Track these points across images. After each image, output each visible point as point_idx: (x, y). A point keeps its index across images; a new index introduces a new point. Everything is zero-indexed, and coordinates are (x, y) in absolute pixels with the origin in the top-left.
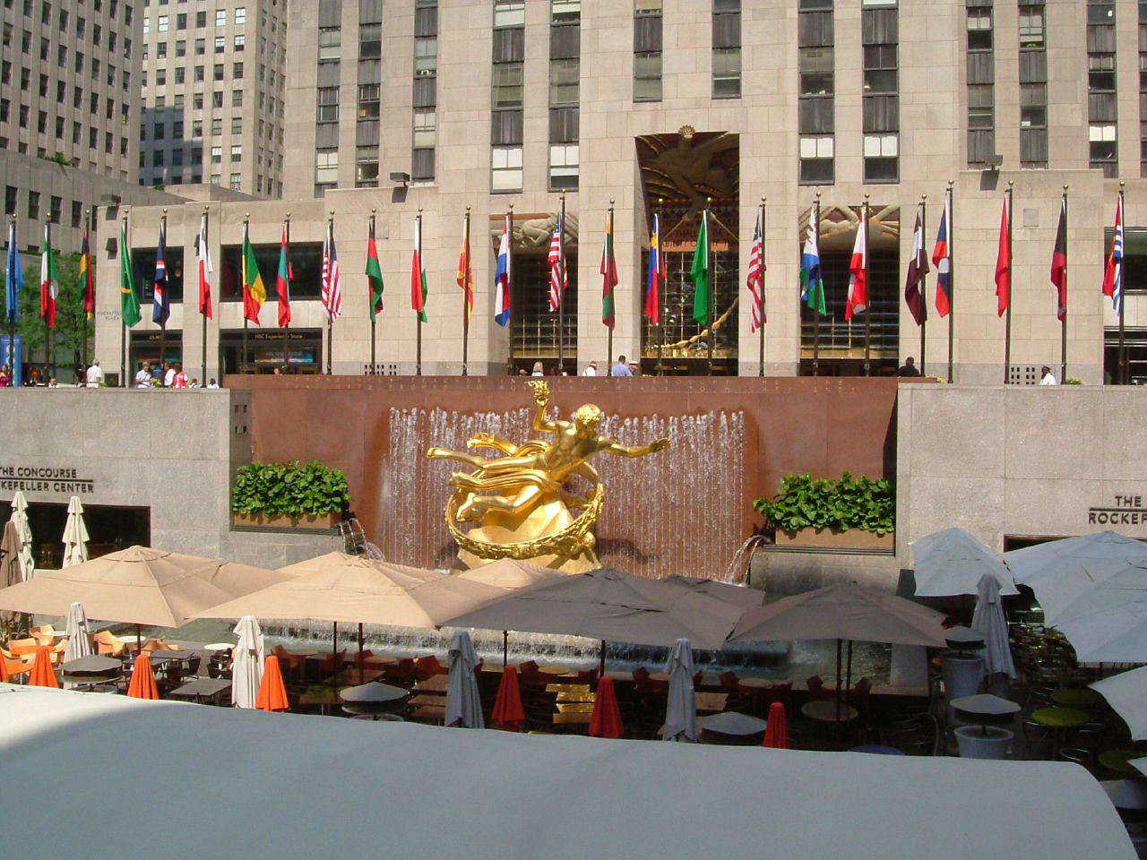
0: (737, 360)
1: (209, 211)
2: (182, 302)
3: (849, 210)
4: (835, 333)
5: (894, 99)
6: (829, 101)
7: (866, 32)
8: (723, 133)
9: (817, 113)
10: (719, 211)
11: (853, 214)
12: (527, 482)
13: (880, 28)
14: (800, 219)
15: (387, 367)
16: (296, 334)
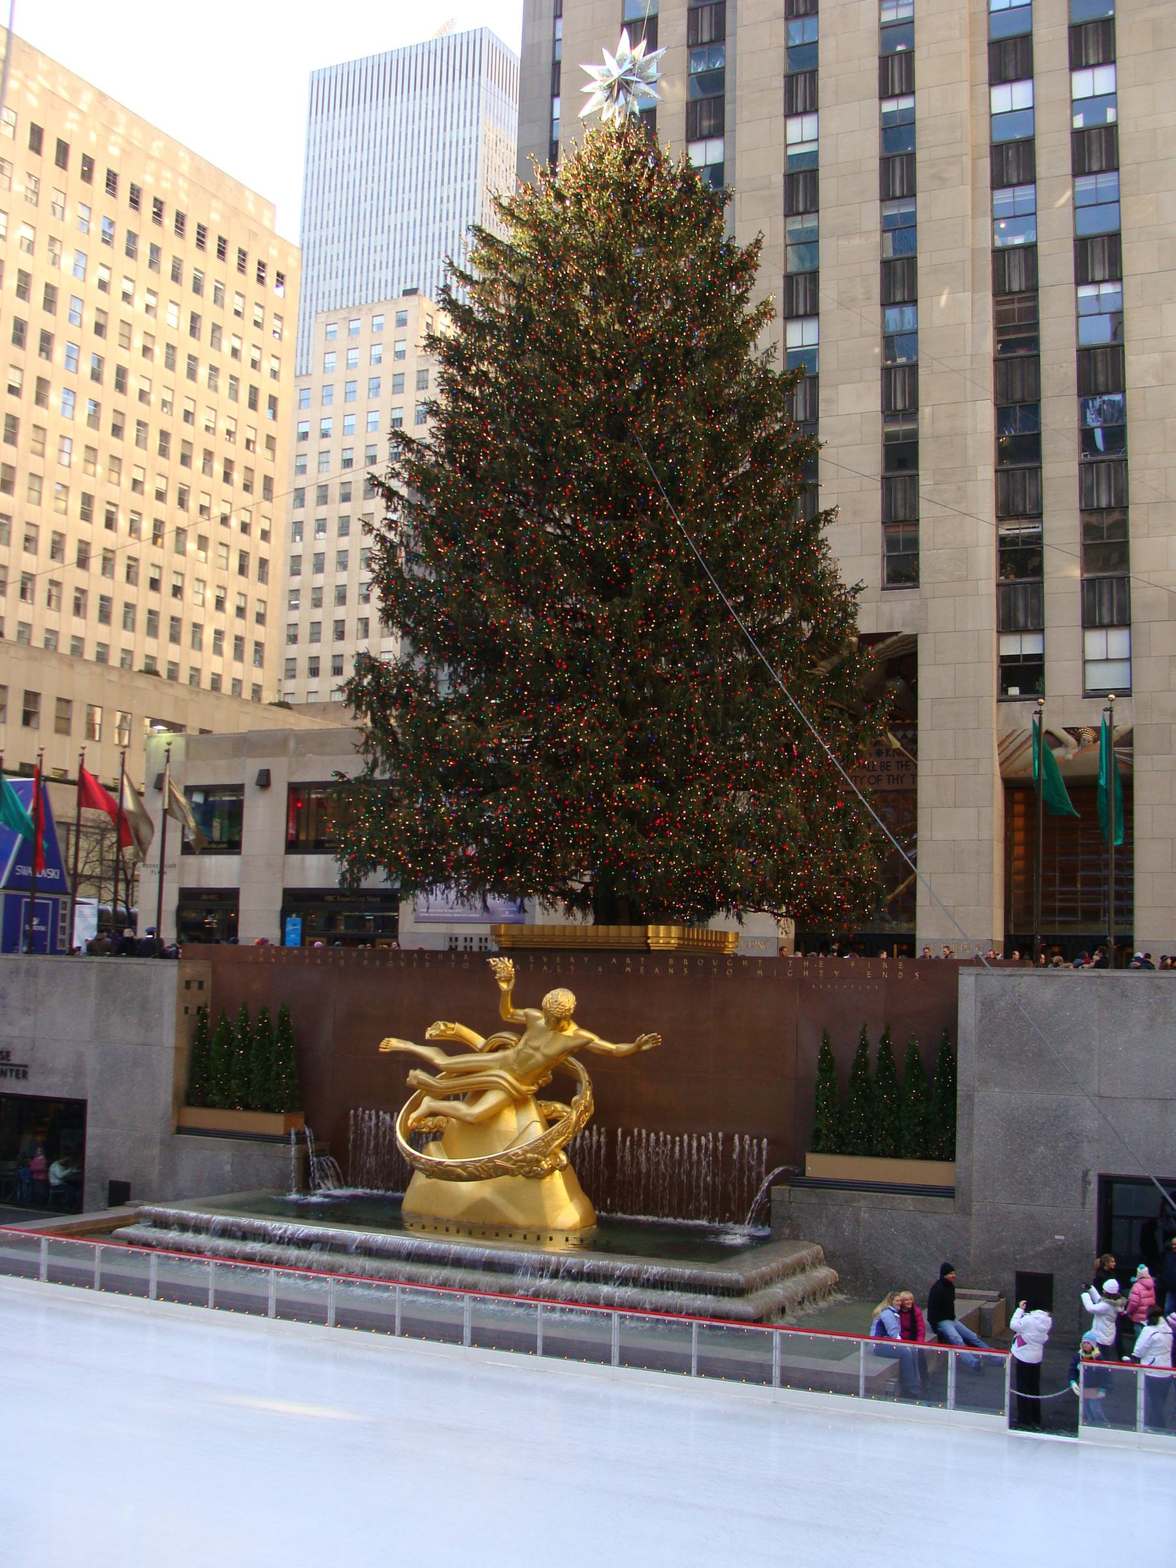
0: (914, 936)
1: (171, 747)
2: (239, 853)
3: (1065, 733)
4: (1061, 900)
5: (1124, 583)
6: (1037, 590)
7: (1086, 492)
8: (896, 633)
9: (1021, 604)
10: (905, 736)
11: (1071, 739)
12: (496, 1086)
13: (1103, 487)
14: (999, 745)
15: (476, 940)
16: (373, 896)
